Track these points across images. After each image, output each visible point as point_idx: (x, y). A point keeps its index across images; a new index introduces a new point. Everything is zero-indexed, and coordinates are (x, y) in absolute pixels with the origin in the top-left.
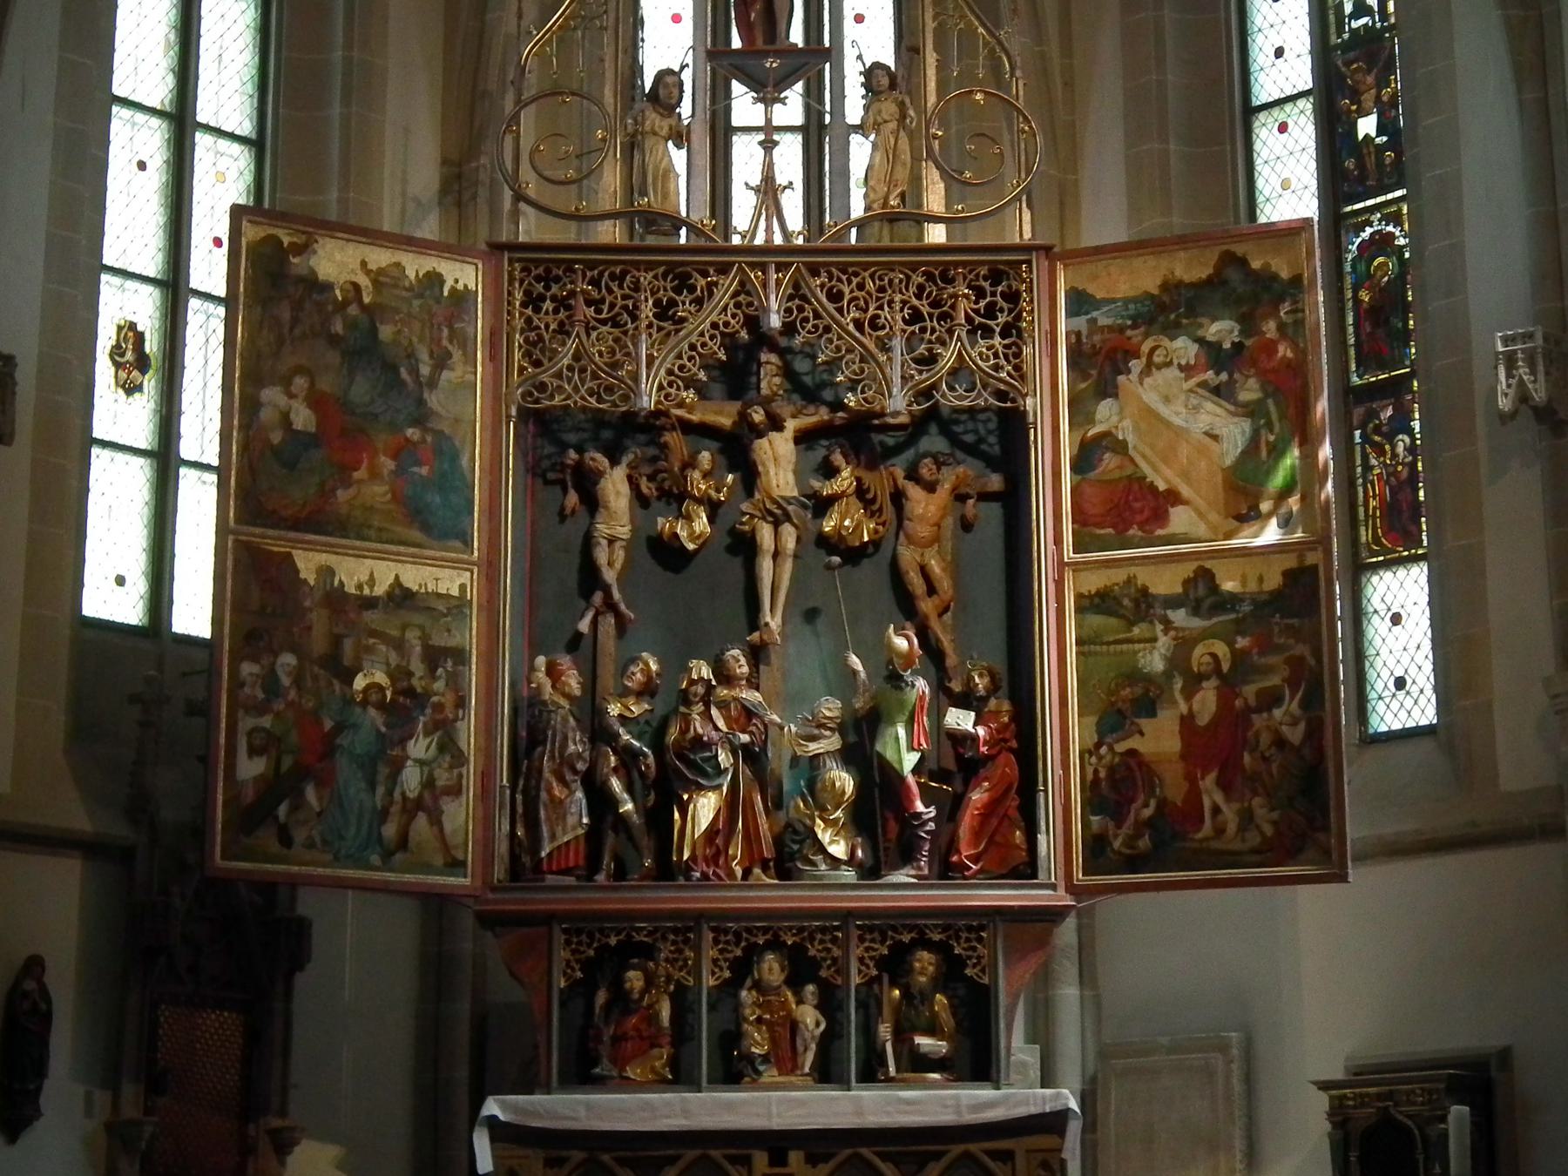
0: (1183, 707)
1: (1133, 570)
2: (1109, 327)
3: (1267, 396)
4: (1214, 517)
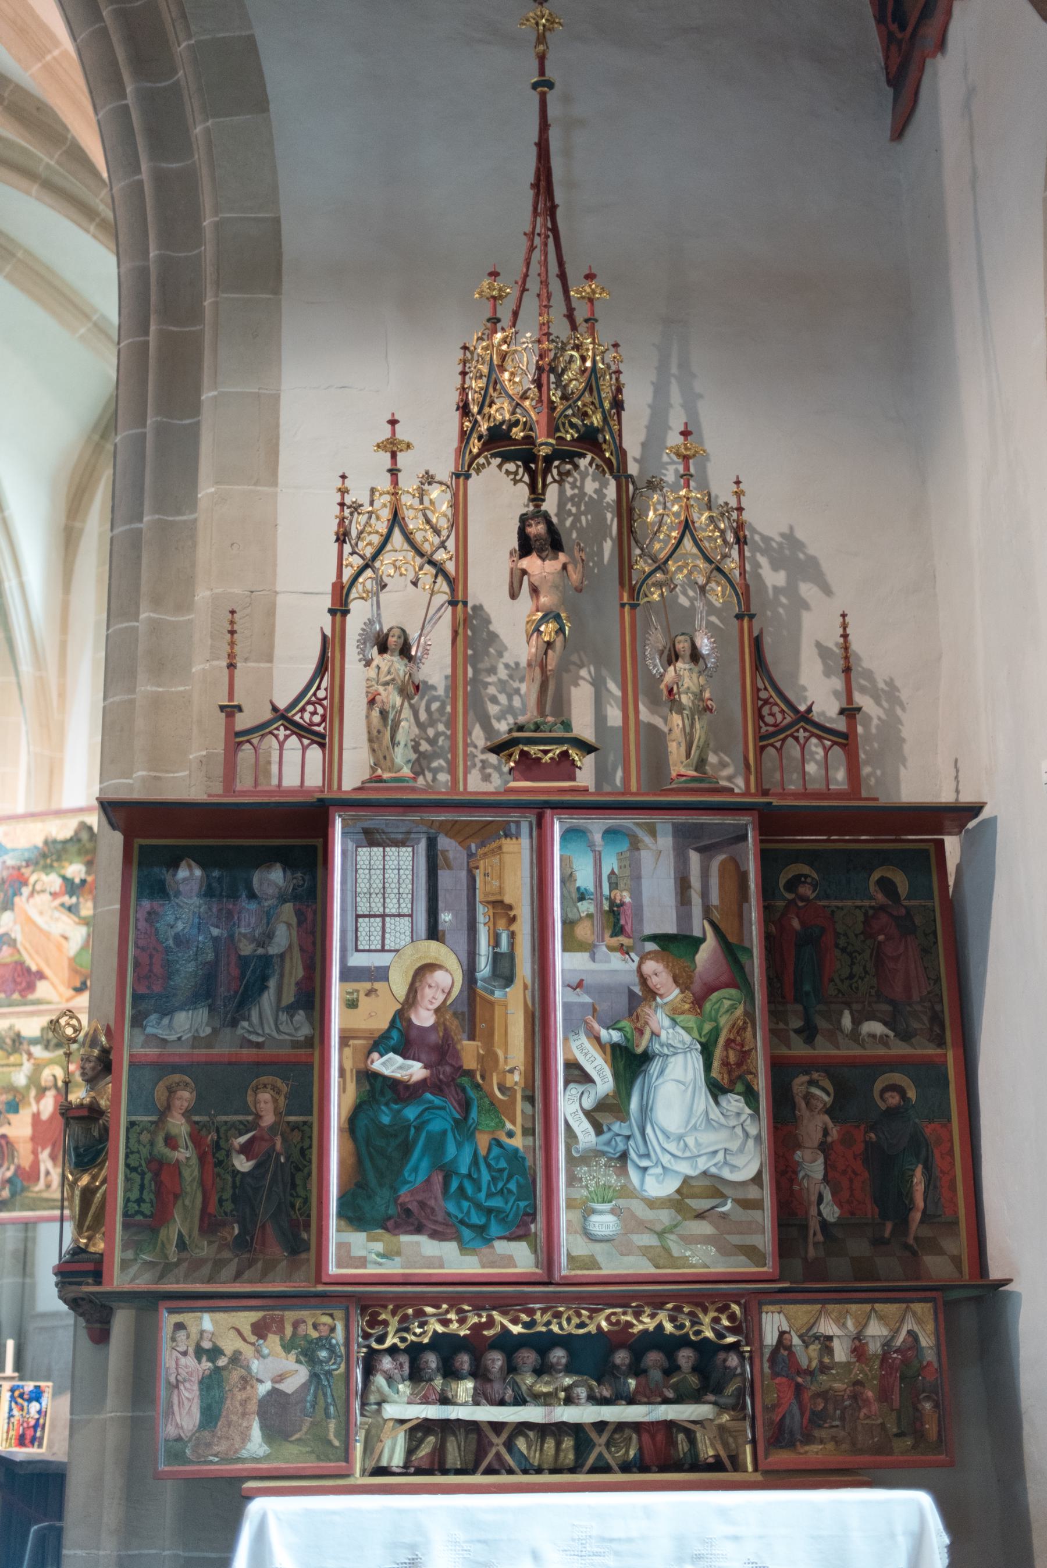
0: (34, 1108)
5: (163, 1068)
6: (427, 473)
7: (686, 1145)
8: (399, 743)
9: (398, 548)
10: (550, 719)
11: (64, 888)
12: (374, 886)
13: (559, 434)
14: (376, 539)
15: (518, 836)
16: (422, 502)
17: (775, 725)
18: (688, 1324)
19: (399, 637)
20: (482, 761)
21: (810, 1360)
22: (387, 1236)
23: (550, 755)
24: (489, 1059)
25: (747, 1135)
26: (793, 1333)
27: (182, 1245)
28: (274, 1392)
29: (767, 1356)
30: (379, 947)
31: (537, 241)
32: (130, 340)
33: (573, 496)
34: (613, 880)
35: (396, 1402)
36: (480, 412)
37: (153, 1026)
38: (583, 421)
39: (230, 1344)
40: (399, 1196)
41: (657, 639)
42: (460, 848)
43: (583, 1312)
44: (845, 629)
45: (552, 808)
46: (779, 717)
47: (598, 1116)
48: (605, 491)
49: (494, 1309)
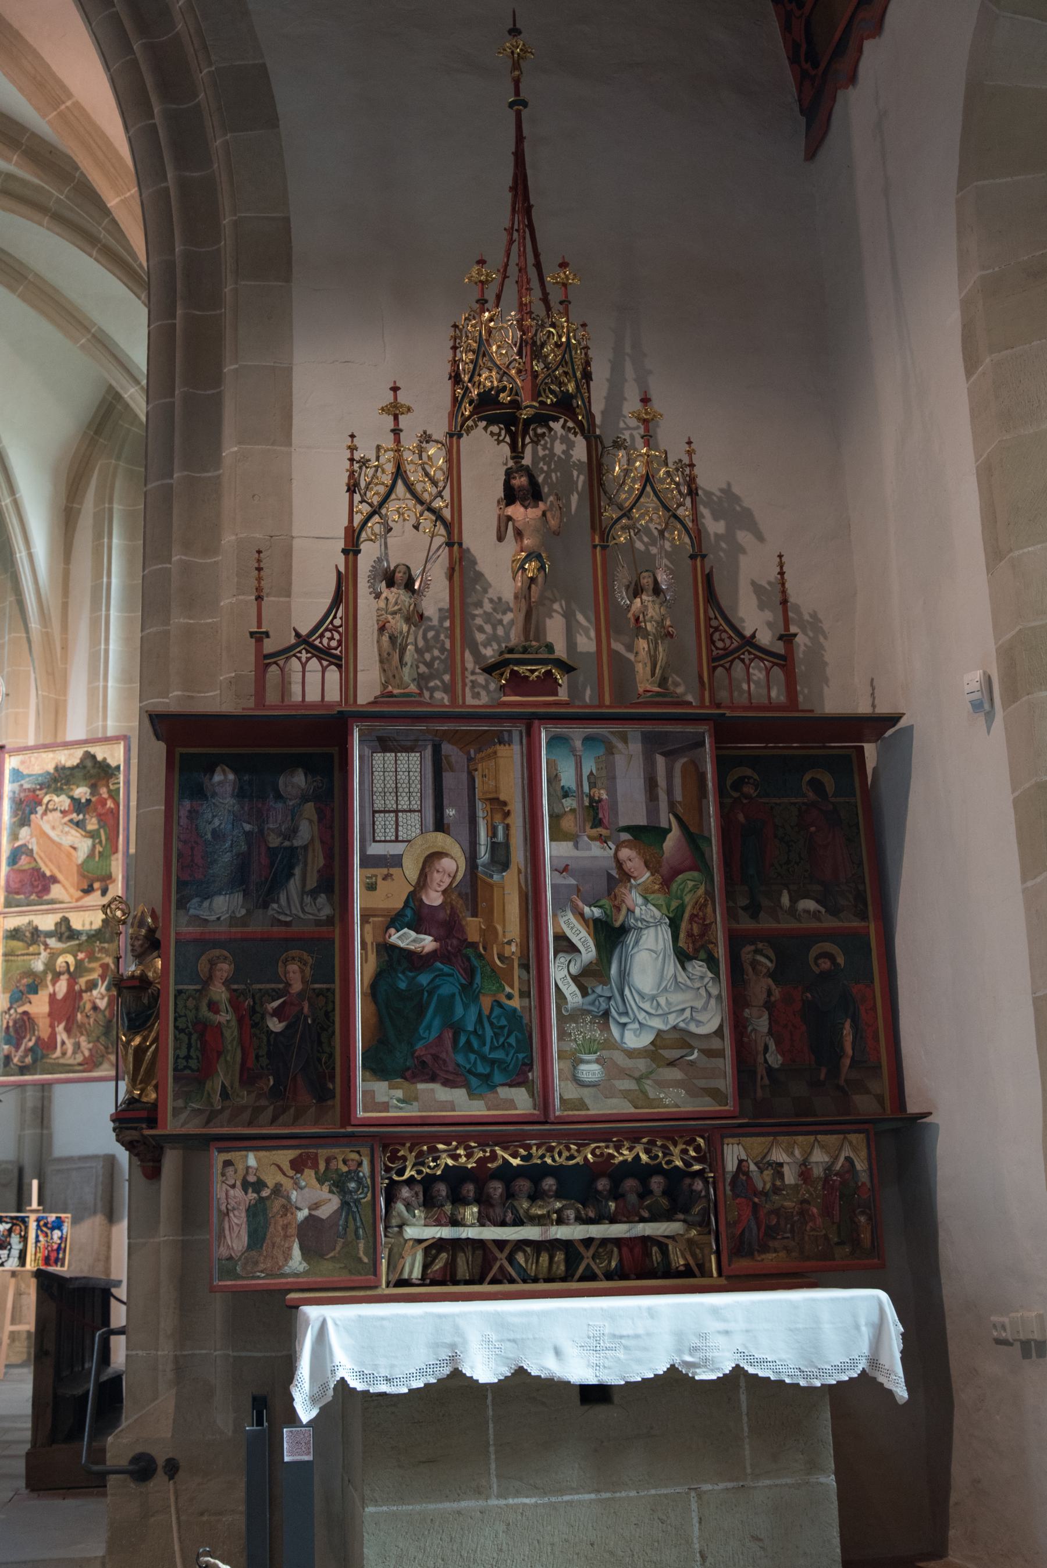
0: (51, 990)
1: (32, 918)
2: (29, 789)
3: (100, 827)
4: (72, 891)
5: (204, 943)
6: (425, 432)
7: (658, 1004)
8: (406, 664)
9: (402, 498)
10: (534, 643)
11: (72, 808)
12: (388, 786)
13: (540, 399)
14: (382, 490)
15: (510, 743)
16: (421, 458)
17: (724, 649)
18: (660, 1155)
19: (405, 573)
20: (472, 681)
21: (765, 1183)
22: (406, 1084)
23: (536, 674)
24: (489, 933)
25: (709, 995)
26: (749, 1161)
27: (225, 1095)
28: (310, 1218)
29: (729, 1180)
30: (393, 838)
31: (515, 235)
32: (159, 323)
33: (545, 456)
34: (592, 780)
35: (414, 1225)
36: (470, 381)
37: (195, 909)
38: (560, 388)
39: (272, 1179)
40: (416, 1050)
41: (623, 576)
42: (461, 753)
43: (572, 1146)
44: (781, 567)
45: (539, 719)
46: (728, 642)
47: (583, 980)
48: (571, 452)
49: (496, 1146)
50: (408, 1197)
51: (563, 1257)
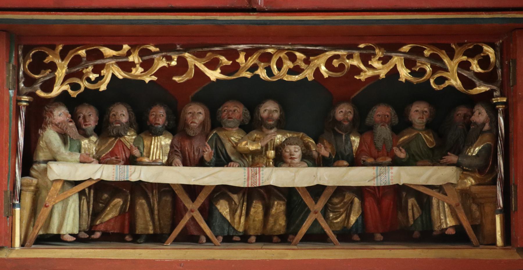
18: (428, 69)
35: (65, 160)
43: (298, 54)
49: (185, 51)
50: (62, 122)
51: (283, 208)
